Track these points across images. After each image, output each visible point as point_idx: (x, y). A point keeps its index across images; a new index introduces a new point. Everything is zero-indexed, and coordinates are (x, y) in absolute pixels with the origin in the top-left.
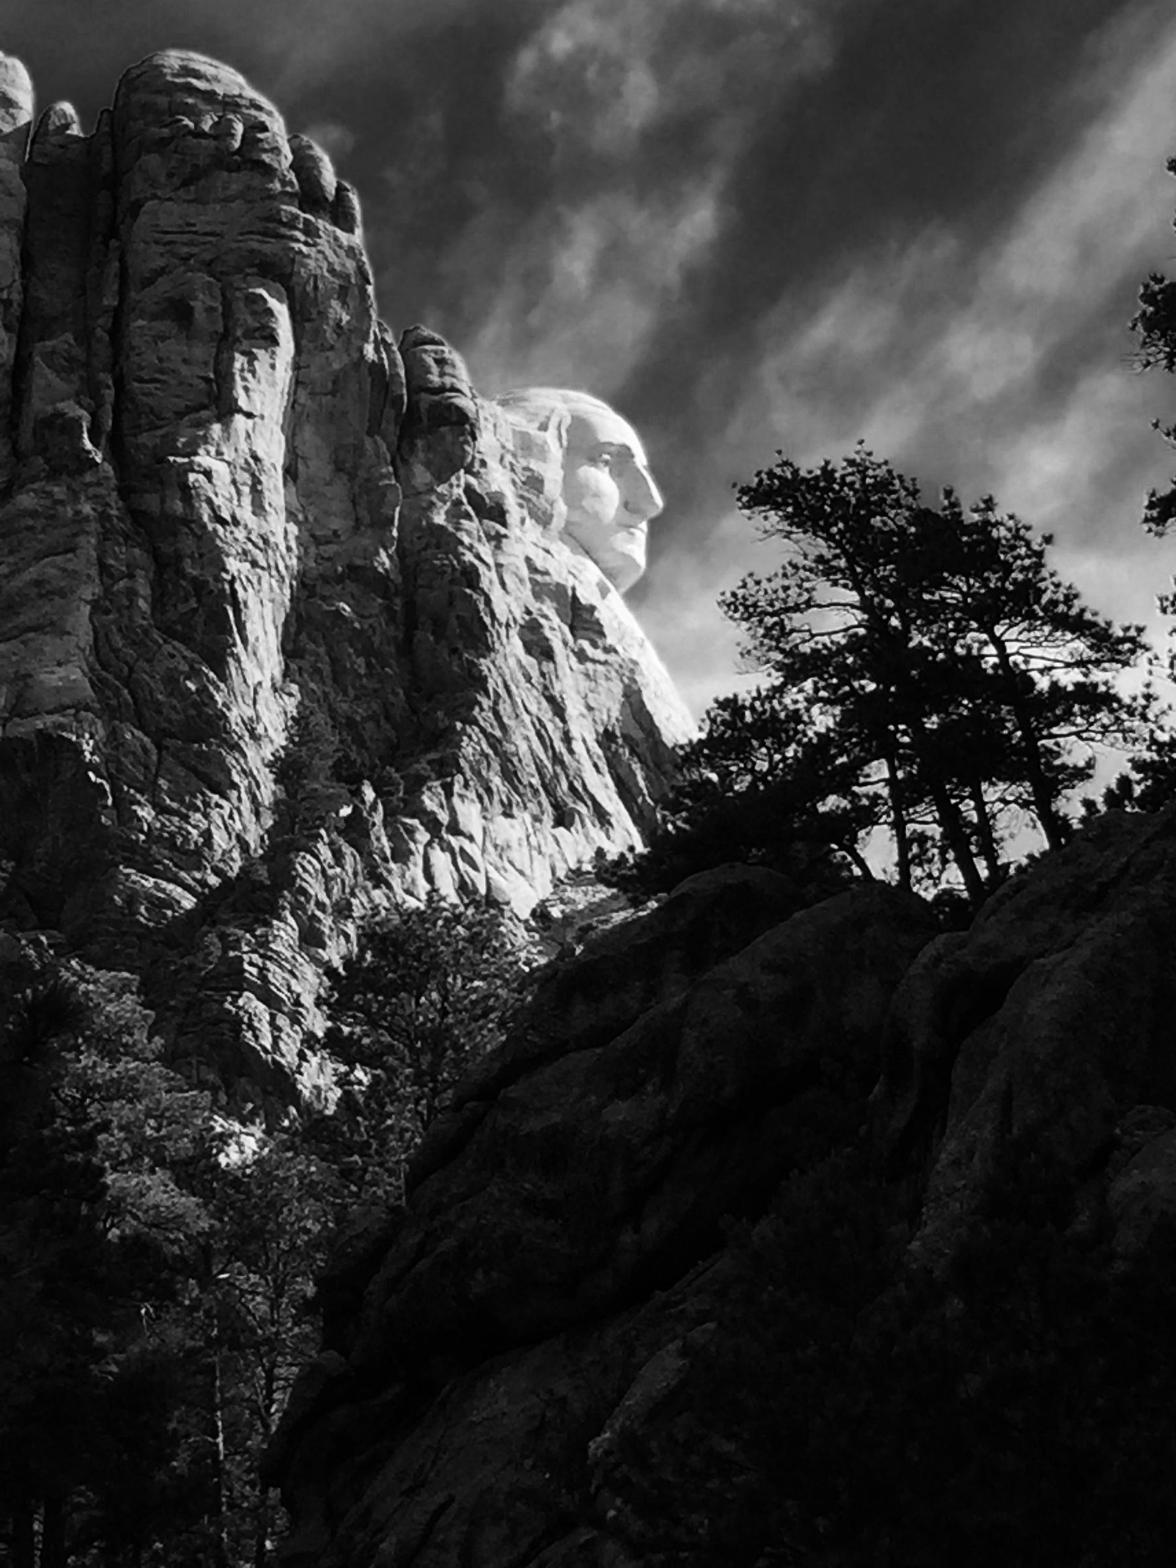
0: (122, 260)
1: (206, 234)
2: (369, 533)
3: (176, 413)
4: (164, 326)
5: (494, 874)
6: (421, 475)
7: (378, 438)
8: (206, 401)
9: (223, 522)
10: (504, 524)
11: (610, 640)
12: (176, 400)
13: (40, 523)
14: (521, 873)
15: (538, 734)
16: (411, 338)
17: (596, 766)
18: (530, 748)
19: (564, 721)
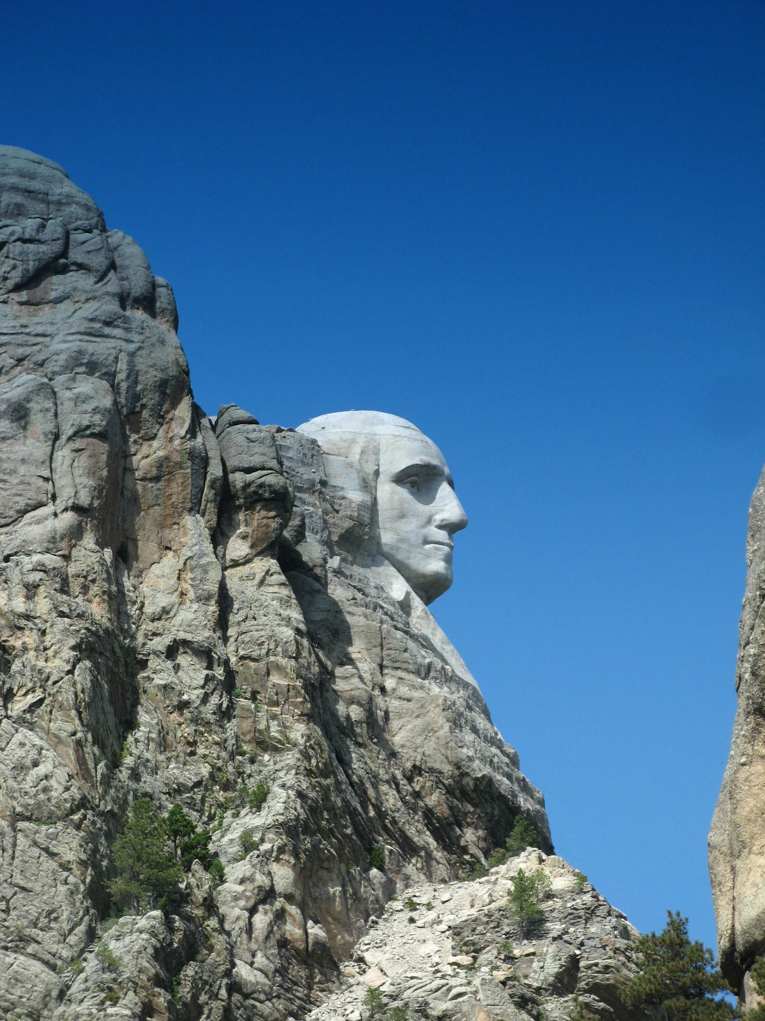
1: (37, 335)
2: (195, 606)
3: (18, 512)
7: (198, 515)
8: (45, 499)
9: (62, 615)
12: (17, 499)
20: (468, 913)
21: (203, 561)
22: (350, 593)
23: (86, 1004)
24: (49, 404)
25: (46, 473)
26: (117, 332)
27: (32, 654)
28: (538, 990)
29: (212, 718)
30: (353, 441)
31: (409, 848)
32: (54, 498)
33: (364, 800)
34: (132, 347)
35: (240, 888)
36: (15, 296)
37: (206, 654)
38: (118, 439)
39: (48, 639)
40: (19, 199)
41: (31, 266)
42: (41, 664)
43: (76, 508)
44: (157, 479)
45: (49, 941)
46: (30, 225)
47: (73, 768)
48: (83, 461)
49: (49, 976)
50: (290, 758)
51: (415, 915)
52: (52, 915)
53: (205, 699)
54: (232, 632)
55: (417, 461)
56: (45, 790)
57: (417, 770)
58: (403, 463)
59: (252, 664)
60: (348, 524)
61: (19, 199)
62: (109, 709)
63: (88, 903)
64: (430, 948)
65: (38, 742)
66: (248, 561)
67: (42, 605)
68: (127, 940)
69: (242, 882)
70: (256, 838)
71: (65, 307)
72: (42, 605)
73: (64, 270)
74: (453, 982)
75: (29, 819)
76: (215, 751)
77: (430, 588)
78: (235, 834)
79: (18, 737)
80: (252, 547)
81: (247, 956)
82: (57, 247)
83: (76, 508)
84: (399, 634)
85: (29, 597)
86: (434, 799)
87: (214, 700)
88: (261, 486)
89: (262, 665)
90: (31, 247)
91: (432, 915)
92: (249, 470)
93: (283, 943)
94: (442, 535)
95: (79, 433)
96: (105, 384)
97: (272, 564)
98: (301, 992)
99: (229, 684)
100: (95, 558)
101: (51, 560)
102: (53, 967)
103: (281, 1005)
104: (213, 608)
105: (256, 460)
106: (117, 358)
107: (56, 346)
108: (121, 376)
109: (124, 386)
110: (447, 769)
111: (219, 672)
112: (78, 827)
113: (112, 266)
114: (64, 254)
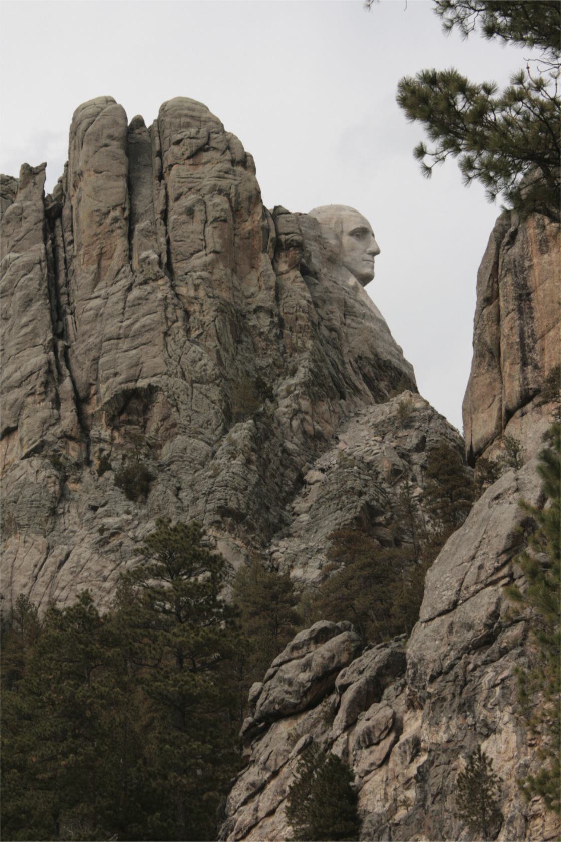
0: (166, 189)
4: (184, 217)
5: (317, 427)
6: (283, 267)
9: (210, 297)
10: (317, 278)
11: (359, 320)
13: (144, 302)
14: (327, 422)
15: (332, 365)
16: (277, 211)
17: (355, 372)
18: (330, 373)
19: (341, 355)
20: (381, 418)
21: (269, 272)
22: (331, 283)
23: (223, 459)
24: (203, 208)
25: (202, 237)
26: (230, 176)
27: (198, 314)
28: (409, 450)
29: (273, 339)
30: (331, 218)
31: (357, 391)
32: (206, 247)
33: (338, 371)
34: (236, 183)
35: (286, 410)
36: (187, 162)
37: (271, 313)
38: (232, 222)
39: (204, 307)
40: (188, 120)
41: (194, 149)
42: (202, 318)
43: (215, 252)
44: (249, 238)
45: (207, 432)
46: (193, 131)
47: (215, 361)
49: (209, 448)
50: (306, 355)
51: (358, 419)
52: (208, 422)
54: (282, 302)
55: (359, 226)
56: (205, 371)
57: (360, 358)
59: (290, 316)
60: (329, 253)
61: (188, 120)
62: (230, 336)
63: (223, 417)
64: (366, 432)
65: (201, 350)
66: (287, 272)
67: (202, 293)
68: (239, 432)
69: (287, 407)
70: (292, 389)
71: (209, 166)
72: (202, 293)
73: (208, 150)
74: (374, 448)
75: (198, 383)
76: (274, 353)
78: (283, 387)
79: (193, 349)
80: (289, 266)
81: (290, 438)
82: (204, 141)
83: (215, 252)
84: (352, 301)
85: (196, 290)
86: (368, 369)
87: (274, 331)
88: (292, 240)
89: (294, 317)
90: (194, 141)
91: (366, 419)
92: (287, 234)
93: (304, 432)
95: (216, 219)
96: (226, 199)
97: (298, 273)
98: (312, 452)
99: (281, 324)
100: (223, 272)
101: (205, 274)
102: (210, 444)
103: (303, 458)
104: (273, 292)
105: (290, 229)
106: (230, 188)
107: (205, 182)
108: (233, 195)
109: (234, 199)
110: (371, 357)
111: (276, 319)
112: (218, 386)
113: (228, 148)
114: (208, 143)
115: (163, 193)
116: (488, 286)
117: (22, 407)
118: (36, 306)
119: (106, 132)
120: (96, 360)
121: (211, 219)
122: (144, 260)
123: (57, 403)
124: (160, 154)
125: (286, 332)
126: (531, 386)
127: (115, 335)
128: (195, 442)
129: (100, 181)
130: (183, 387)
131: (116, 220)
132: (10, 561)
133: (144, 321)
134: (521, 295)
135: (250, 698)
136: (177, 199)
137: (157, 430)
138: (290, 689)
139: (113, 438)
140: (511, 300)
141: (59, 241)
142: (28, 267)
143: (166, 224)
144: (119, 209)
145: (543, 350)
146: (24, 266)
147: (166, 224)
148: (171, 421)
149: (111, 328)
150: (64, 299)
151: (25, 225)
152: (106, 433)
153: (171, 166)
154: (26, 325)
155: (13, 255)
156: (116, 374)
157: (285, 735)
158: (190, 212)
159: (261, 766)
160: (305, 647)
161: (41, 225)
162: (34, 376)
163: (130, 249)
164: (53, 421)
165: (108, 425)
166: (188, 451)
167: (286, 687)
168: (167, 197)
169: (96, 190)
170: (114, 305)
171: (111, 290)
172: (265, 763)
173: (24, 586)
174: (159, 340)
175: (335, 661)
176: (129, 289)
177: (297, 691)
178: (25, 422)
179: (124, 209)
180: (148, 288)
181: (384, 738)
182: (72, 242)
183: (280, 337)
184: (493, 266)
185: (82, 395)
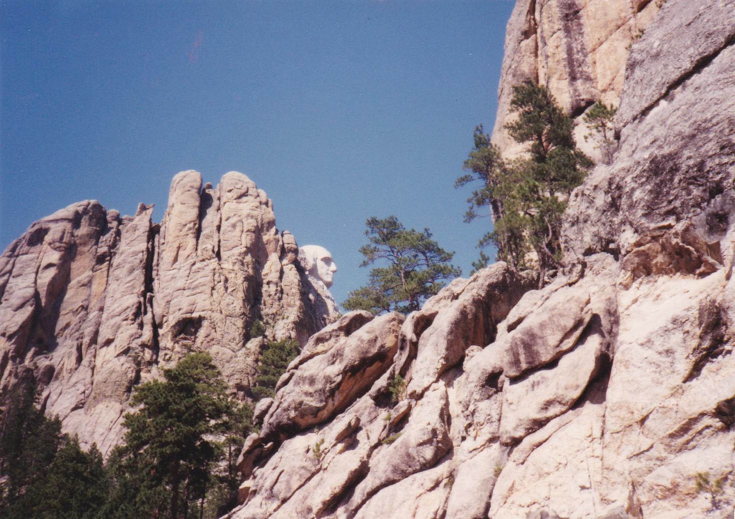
4: (230, 228)
41: (239, 194)
46: (239, 186)
47: (242, 305)
48: (249, 237)
53: (276, 294)
58: (323, 256)
73: (247, 196)
77: (328, 285)
82: (245, 190)
83: (246, 247)
94: (331, 273)
95: (248, 231)
99: (282, 292)
101: (240, 258)
111: (279, 289)
114: (247, 192)
115: (219, 216)
116: (526, 20)
117: (119, 327)
118: (137, 272)
119: (190, 184)
120: (168, 302)
121: (245, 230)
122: (204, 249)
123: (141, 326)
124: (219, 199)
125: (285, 296)
126: (584, 97)
127: (182, 287)
128: (225, 349)
129: (183, 208)
130: (220, 318)
131: (190, 229)
132: (96, 418)
133: (200, 280)
134: (567, 15)
135: (257, 412)
136: (227, 220)
137: (202, 343)
138: (311, 390)
139: (173, 348)
140: (556, 21)
141: (156, 243)
142: (135, 254)
143: (219, 232)
144: (193, 223)
145: (595, 63)
146: (132, 253)
147: (219, 232)
148: (210, 337)
149: (180, 283)
150: (154, 273)
151: (137, 233)
152: (170, 344)
153: (225, 203)
154: (129, 282)
155: (127, 248)
156: (180, 310)
157: (302, 450)
158: (234, 226)
159: (265, 495)
160: (333, 340)
161: (146, 234)
162: (129, 309)
163: (197, 245)
164: (137, 336)
165: (172, 340)
166: (220, 354)
167: (307, 388)
168: (221, 219)
169: (181, 213)
170: (184, 272)
171: (182, 265)
172: (272, 488)
173: (102, 434)
174: (209, 291)
175: (378, 344)
176: (194, 264)
177: (322, 391)
178: (120, 336)
179: (195, 224)
180: (204, 263)
181: (571, 350)
182: (164, 243)
183: (280, 299)
184: (531, 4)
185: (157, 322)
